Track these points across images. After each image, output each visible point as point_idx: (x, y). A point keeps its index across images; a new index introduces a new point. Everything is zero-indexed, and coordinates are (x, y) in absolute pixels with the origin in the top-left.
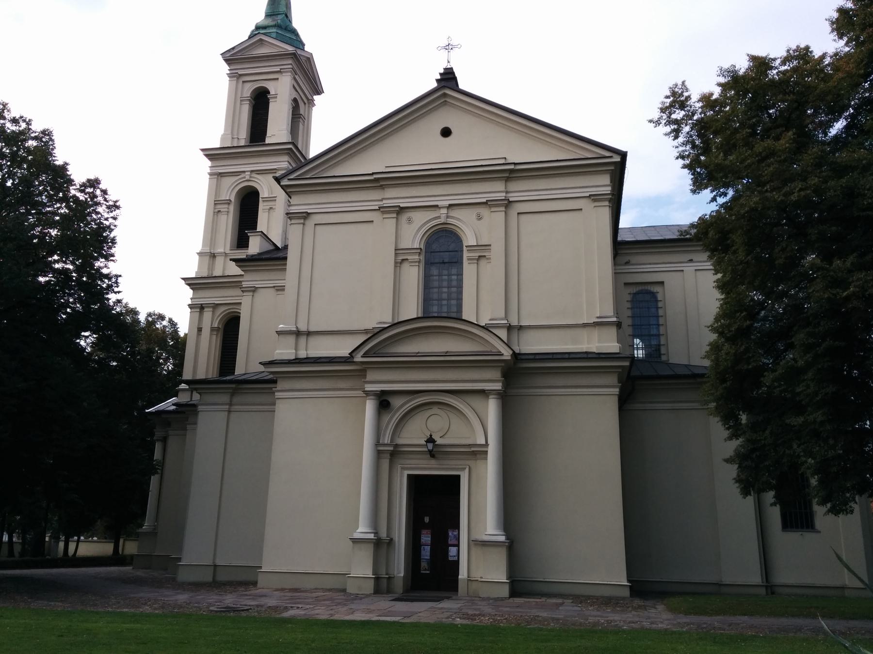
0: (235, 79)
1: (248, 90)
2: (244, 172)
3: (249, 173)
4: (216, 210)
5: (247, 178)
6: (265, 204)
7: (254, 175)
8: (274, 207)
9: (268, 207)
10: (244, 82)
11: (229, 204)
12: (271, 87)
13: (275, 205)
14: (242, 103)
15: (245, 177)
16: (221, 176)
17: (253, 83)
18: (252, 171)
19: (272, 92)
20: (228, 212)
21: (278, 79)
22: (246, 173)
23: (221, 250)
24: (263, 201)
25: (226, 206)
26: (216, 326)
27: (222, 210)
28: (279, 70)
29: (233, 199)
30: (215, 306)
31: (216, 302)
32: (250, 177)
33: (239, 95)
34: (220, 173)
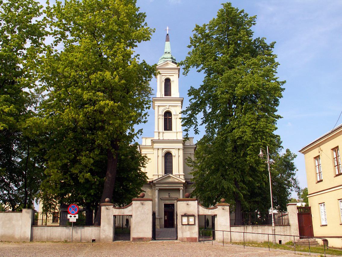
1: (164, 78)
12: (172, 78)
19: (172, 80)
21: (173, 76)
30: (163, 149)
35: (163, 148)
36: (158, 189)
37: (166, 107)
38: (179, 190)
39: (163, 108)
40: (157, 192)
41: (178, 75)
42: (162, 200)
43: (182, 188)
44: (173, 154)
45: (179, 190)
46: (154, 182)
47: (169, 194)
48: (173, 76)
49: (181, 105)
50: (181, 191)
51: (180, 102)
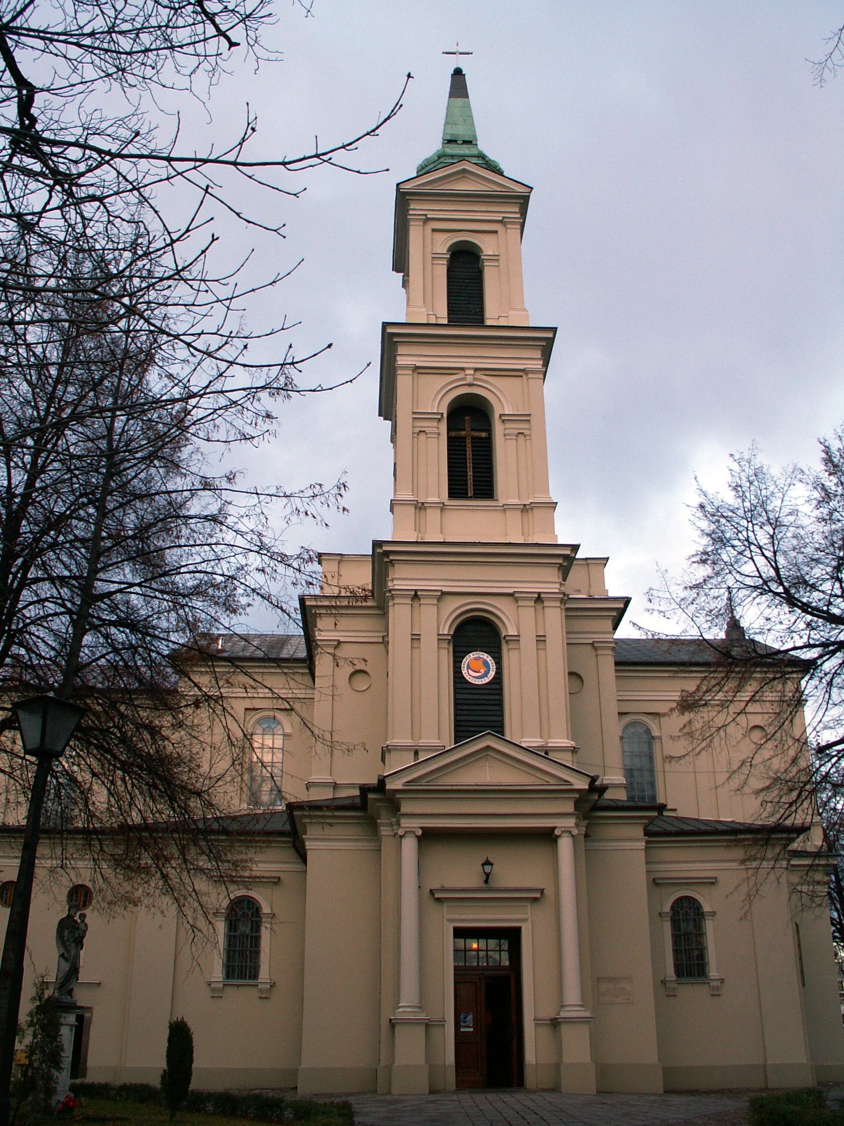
0: (421, 223)
1: (443, 244)
2: (463, 369)
3: (472, 372)
4: (417, 430)
5: (469, 379)
6: (508, 425)
7: (479, 375)
8: (526, 432)
9: (516, 431)
10: (434, 230)
11: (439, 420)
14: (435, 262)
15: (464, 379)
16: (418, 373)
17: (449, 234)
18: (476, 370)
20: (439, 434)
21: (496, 232)
22: (468, 372)
23: (436, 500)
24: (503, 421)
25: (435, 424)
26: (446, 632)
27: (427, 430)
28: (501, 218)
29: (445, 415)
31: (445, 589)
33: (428, 250)
35: (444, 593)
36: (420, 832)
37: (461, 375)
38: (548, 837)
39: (443, 380)
40: (409, 846)
41: (519, 231)
42: (439, 900)
43: (570, 822)
44: (509, 629)
45: (548, 837)
46: (389, 786)
47: (488, 863)
48: (496, 232)
49: (543, 365)
50: (565, 845)
51: (538, 354)
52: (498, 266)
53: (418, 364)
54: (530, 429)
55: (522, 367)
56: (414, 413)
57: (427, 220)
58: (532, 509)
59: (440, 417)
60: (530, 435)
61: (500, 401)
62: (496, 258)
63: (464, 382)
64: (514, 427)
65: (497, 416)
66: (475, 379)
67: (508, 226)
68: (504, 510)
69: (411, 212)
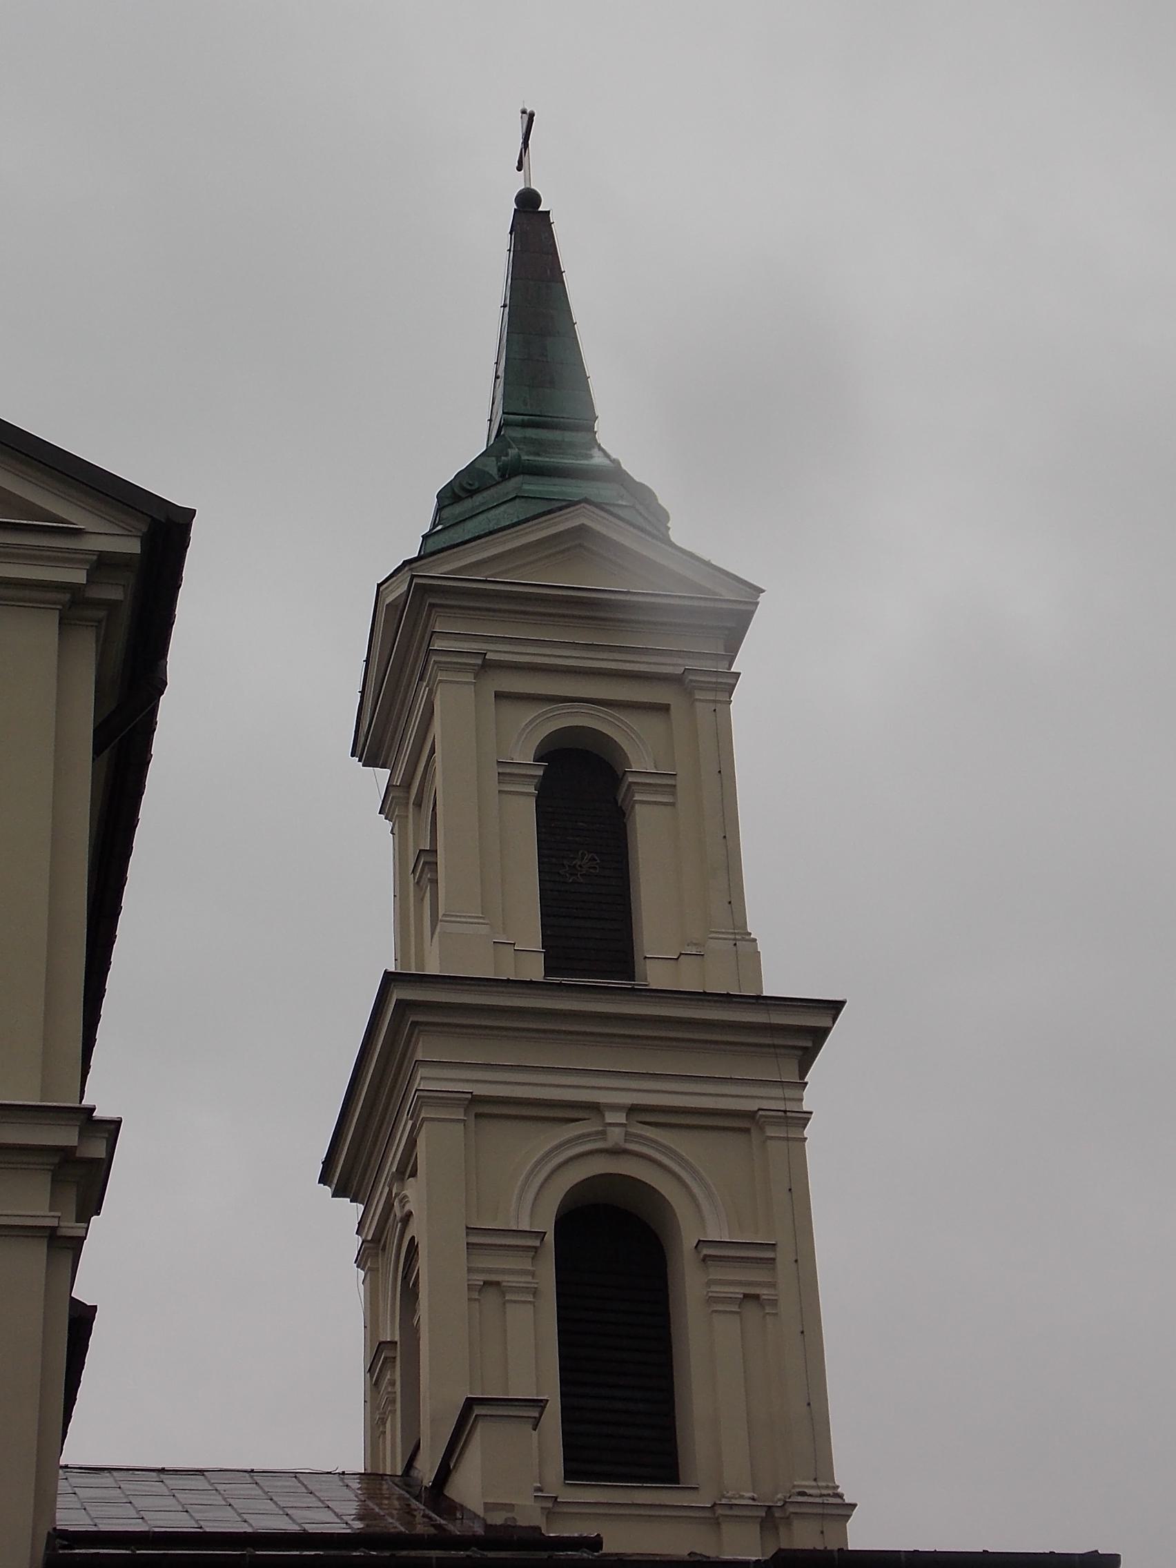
3: (621, 1118)
4: (479, 1279)
5: (615, 1137)
6: (717, 1273)
8: (764, 1292)
9: (739, 1291)
10: (499, 696)
13: (773, 1285)
16: (478, 1116)
18: (633, 1110)
21: (664, 709)
22: (610, 1118)
24: (706, 1258)
28: (680, 670)
29: (550, 1238)
32: (628, 1136)
34: (476, 1100)
48: (663, 709)
52: (673, 804)
53: (480, 1090)
54: (773, 1285)
55: (752, 1106)
56: (470, 1230)
57: (487, 666)
58: (788, 1520)
59: (537, 1243)
60: (774, 1303)
61: (698, 1206)
62: (666, 784)
63: (599, 1145)
64: (733, 1280)
65: (689, 1242)
66: (628, 1136)
67: (699, 695)
68: (716, 1523)
69: (438, 645)
